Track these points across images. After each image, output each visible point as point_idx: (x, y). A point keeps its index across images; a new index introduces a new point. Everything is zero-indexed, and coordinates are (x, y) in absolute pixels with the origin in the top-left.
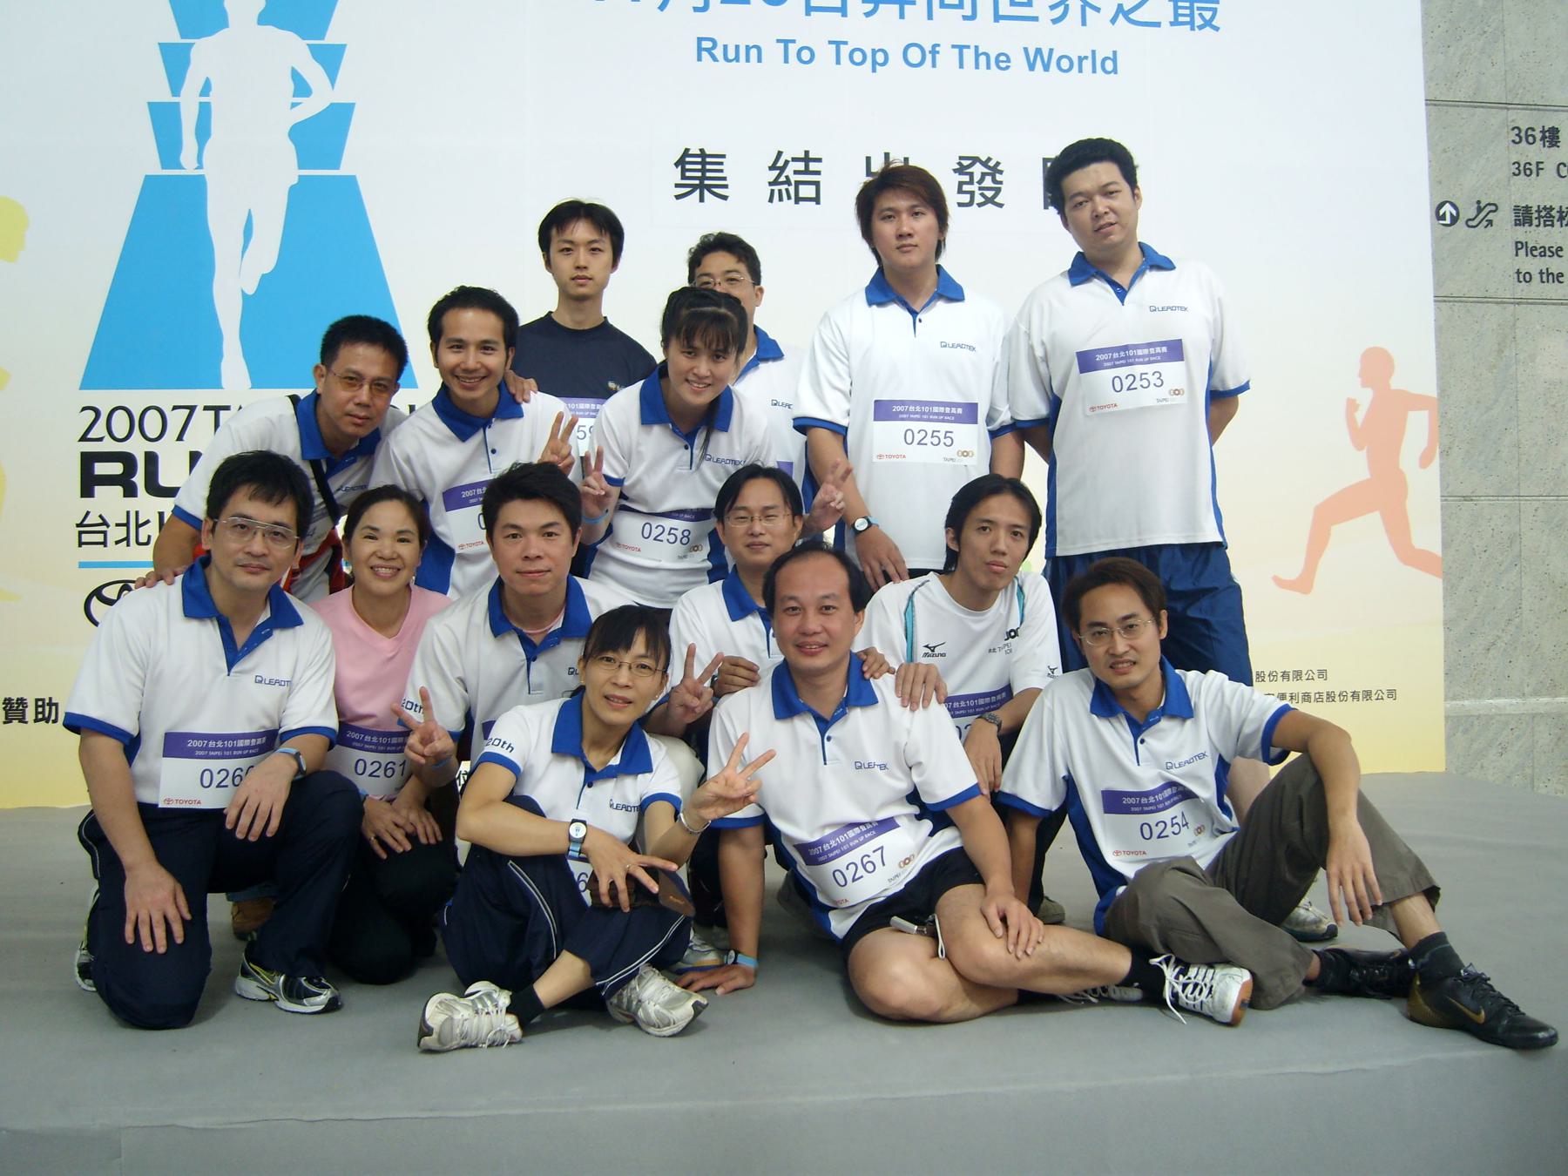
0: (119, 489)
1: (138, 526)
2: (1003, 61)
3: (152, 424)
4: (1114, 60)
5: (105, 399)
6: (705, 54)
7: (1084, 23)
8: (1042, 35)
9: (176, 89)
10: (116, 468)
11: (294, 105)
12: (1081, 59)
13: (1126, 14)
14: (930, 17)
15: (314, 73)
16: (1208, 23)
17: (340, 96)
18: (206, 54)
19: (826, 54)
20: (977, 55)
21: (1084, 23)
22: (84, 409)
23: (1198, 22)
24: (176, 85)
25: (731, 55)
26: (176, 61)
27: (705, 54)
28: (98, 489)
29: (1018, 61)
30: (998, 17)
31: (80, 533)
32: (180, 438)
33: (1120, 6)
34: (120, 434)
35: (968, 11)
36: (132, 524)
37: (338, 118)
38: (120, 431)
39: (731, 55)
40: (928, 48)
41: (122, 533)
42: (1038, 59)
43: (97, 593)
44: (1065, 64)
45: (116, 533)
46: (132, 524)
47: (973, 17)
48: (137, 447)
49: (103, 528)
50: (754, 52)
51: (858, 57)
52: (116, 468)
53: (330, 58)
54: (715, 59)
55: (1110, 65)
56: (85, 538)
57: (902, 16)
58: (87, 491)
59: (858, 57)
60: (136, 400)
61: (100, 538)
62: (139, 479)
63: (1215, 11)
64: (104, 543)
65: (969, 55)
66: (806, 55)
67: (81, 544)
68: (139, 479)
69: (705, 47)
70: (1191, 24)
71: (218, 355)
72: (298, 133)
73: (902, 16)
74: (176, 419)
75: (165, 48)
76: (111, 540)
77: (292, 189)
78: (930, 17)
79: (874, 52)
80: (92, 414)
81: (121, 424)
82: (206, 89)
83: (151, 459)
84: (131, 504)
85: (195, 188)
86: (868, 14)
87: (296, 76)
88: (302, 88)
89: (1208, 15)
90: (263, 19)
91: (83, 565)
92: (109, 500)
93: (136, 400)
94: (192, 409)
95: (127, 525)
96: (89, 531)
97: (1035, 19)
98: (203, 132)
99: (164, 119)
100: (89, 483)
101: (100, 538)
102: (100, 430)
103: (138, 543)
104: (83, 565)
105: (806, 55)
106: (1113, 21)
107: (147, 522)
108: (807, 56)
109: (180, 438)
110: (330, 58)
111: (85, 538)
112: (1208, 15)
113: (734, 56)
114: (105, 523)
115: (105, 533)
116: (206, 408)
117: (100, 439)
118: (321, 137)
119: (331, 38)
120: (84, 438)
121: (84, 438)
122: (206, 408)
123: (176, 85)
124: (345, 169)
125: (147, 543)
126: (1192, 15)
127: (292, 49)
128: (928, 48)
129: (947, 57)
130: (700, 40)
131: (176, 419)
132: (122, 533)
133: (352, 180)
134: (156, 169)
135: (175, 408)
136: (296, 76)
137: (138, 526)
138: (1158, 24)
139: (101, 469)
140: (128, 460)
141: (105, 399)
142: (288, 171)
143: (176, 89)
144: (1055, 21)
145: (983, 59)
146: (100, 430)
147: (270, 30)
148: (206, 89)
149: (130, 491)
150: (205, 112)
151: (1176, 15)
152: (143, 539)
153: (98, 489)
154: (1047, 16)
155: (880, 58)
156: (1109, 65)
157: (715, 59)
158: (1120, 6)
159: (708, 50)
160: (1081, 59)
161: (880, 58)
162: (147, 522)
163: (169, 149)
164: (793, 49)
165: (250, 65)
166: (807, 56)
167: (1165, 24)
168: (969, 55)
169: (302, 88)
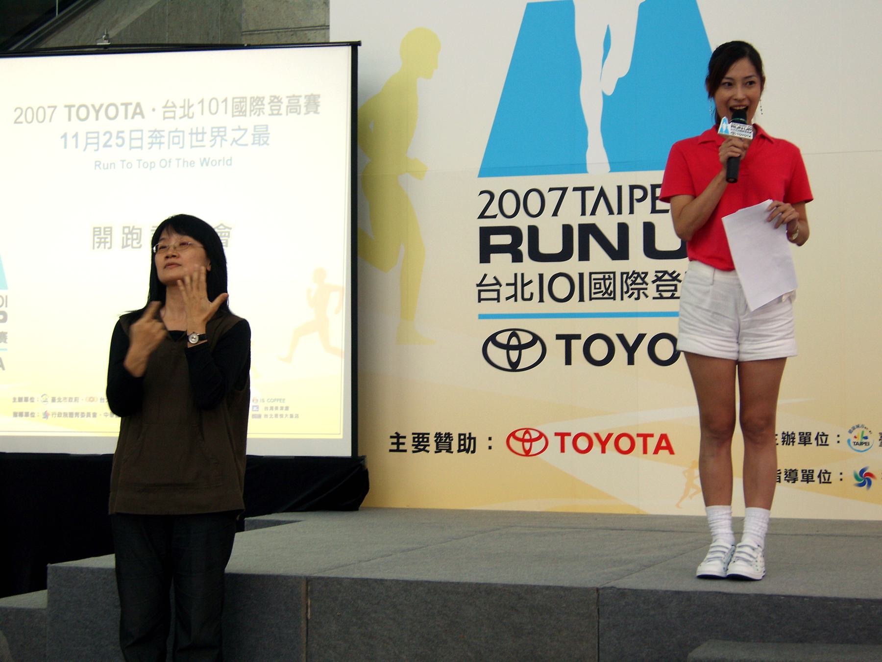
0: (509, 256)
1: (523, 285)
3: (534, 203)
5: (497, 185)
10: (506, 239)
22: (482, 193)
28: (493, 256)
31: (480, 291)
32: (555, 214)
36: (519, 283)
38: (509, 210)
41: (511, 291)
43: (492, 339)
48: (522, 222)
49: (497, 287)
52: (506, 240)
56: (484, 295)
58: (485, 258)
60: (521, 184)
61: (494, 295)
62: (524, 248)
64: (498, 299)
67: (480, 300)
68: (524, 248)
74: (552, 199)
80: (487, 197)
81: (509, 204)
83: (534, 231)
84: (518, 268)
91: (482, 317)
92: (501, 264)
93: (521, 184)
94: (564, 190)
95: (515, 284)
96: (486, 289)
100: (486, 252)
101: (494, 295)
102: (494, 209)
103: (523, 299)
104: (482, 317)
107: (531, 282)
109: (555, 214)
111: (484, 295)
114: (498, 283)
115: (498, 291)
116: (575, 189)
117: (495, 217)
120: (482, 216)
121: (482, 216)
122: (575, 189)
131: (552, 199)
132: (511, 291)
135: (551, 190)
139: (495, 240)
140: (515, 232)
141: (497, 185)
146: (494, 209)
149: (517, 258)
152: (527, 296)
153: (493, 256)
162: (531, 282)
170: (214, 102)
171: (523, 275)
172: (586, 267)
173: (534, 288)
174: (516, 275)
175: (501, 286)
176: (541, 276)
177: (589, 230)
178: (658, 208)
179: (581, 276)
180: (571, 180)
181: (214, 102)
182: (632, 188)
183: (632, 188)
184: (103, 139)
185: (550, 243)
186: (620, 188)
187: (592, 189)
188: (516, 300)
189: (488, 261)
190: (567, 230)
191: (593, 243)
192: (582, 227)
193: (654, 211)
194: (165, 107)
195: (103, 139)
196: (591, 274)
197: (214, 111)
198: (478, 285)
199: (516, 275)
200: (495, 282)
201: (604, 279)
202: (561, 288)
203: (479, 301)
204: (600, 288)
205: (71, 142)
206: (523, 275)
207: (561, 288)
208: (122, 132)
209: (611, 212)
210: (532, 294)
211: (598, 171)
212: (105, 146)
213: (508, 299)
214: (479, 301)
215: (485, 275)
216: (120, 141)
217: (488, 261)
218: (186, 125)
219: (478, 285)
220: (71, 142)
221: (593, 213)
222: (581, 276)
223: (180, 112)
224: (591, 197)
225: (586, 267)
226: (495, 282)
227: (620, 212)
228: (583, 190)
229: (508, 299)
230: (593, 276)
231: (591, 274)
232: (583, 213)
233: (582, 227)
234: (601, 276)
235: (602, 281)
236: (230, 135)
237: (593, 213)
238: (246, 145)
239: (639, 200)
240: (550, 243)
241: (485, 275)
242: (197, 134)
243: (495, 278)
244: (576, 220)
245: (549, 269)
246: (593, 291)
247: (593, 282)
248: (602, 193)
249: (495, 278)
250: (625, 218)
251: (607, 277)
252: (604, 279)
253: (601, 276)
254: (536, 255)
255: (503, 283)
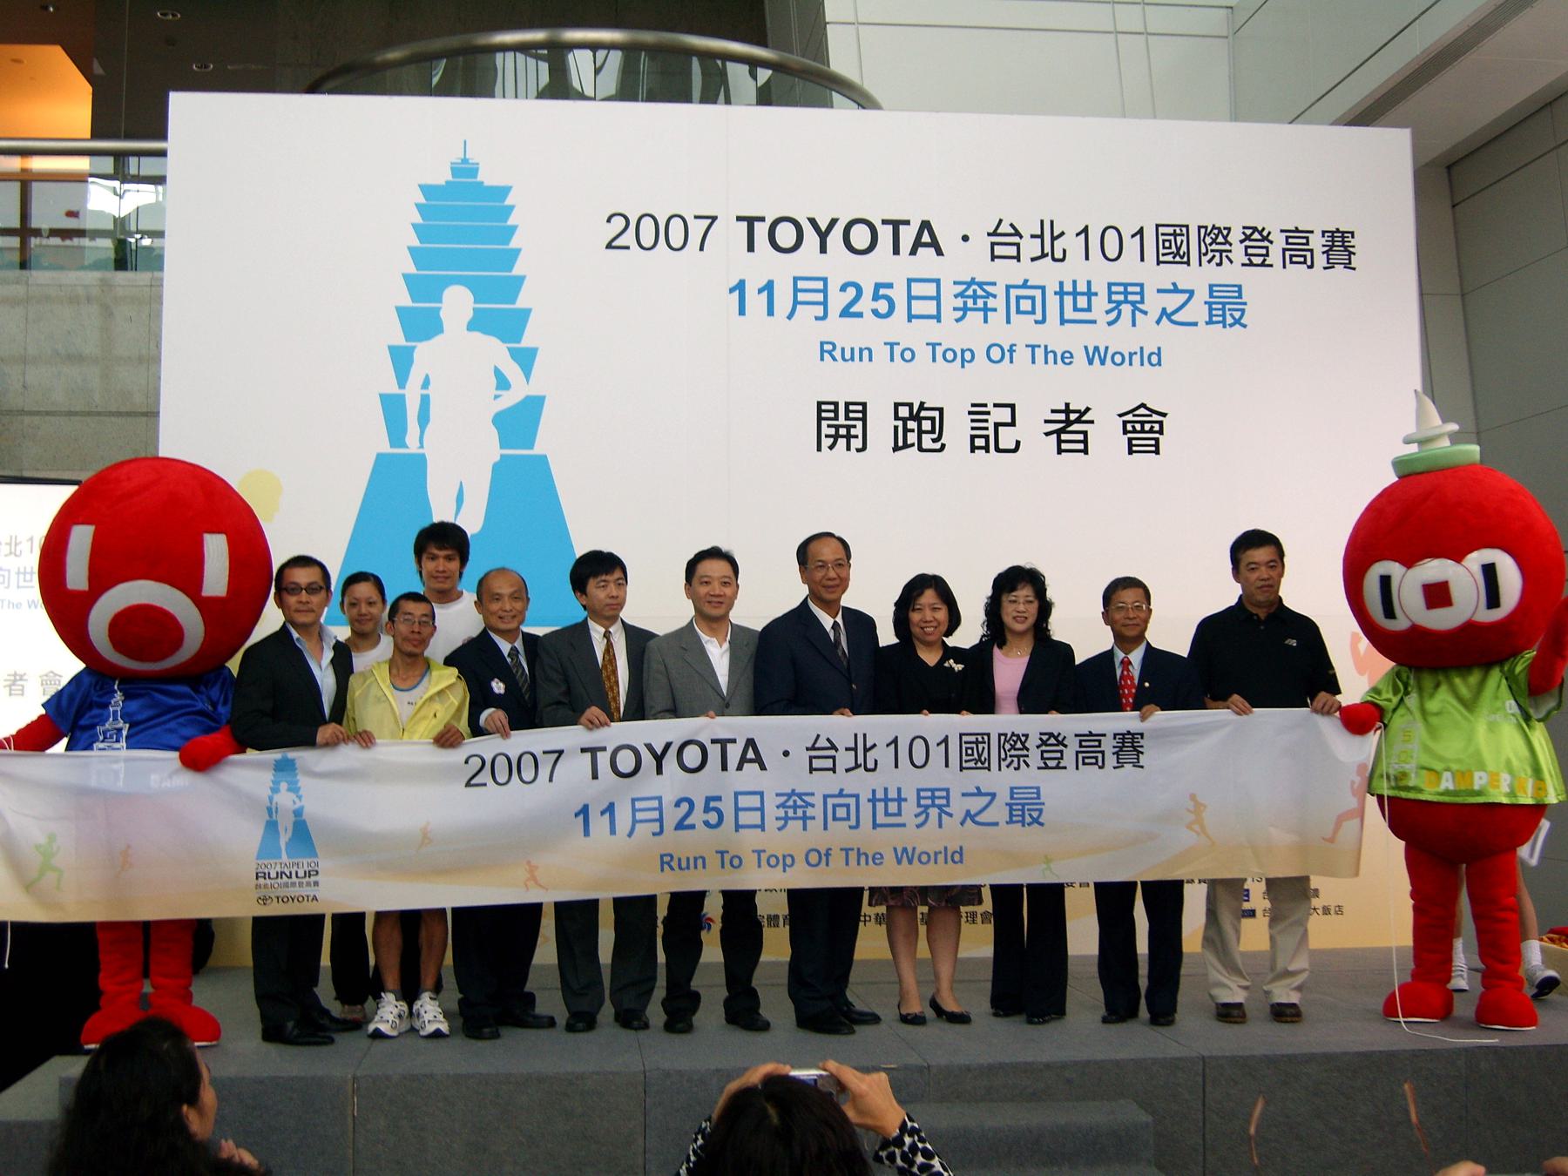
2: (1066, 358)
4: (1159, 355)
6: (826, 355)
7: (1134, 324)
8: (1099, 335)
9: (402, 385)
11: (496, 397)
12: (1131, 355)
13: (1169, 317)
14: (1008, 322)
15: (512, 371)
16: (1237, 322)
17: (533, 389)
18: (426, 354)
19: (924, 353)
20: (1046, 353)
21: (1134, 324)
23: (1229, 320)
24: (402, 381)
25: (848, 356)
26: (402, 360)
27: (826, 355)
29: (1080, 357)
30: (1063, 321)
33: (1164, 310)
35: (1039, 316)
37: (533, 406)
39: (848, 356)
40: (1006, 348)
42: (1096, 355)
44: (1118, 359)
47: (1043, 321)
50: (866, 353)
51: (950, 356)
53: (526, 359)
54: (834, 359)
55: (1155, 358)
57: (986, 321)
59: (950, 356)
63: (1243, 311)
65: (1040, 353)
66: (908, 355)
69: (827, 350)
70: (1224, 323)
72: (500, 420)
73: (986, 321)
75: (393, 350)
77: (495, 466)
78: (1008, 322)
79: (963, 351)
82: (426, 383)
85: (418, 464)
86: (957, 321)
87: (497, 372)
88: (503, 383)
89: (1237, 314)
90: (471, 326)
97: (1094, 322)
98: (424, 419)
99: (393, 408)
105: (908, 355)
106: (1158, 322)
108: (909, 356)
110: (526, 359)
112: (1237, 314)
113: (850, 356)
118: (519, 423)
119: (527, 342)
123: (402, 381)
124: (537, 450)
126: (1224, 316)
127: (494, 351)
128: (1006, 348)
129: (1022, 354)
130: (822, 344)
133: (542, 460)
134: (386, 448)
136: (497, 372)
138: (1195, 324)
142: (490, 449)
143: (402, 385)
144: (1110, 324)
145: (1051, 356)
147: (477, 335)
148: (426, 383)
150: (425, 400)
151: (1211, 315)
154: (1103, 319)
155: (968, 356)
156: (1154, 359)
157: (834, 359)
158: (1164, 310)
159: (830, 352)
160: (1131, 355)
161: (968, 356)
163: (396, 431)
164: (898, 351)
165: (461, 363)
166: (909, 356)
167: (1202, 324)
168: (1040, 353)
169: (503, 383)
170: (1111, 234)
181: (1111, 234)
184: (838, 301)
194: (994, 234)
195: (838, 301)
197: (1112, 254)
205: (756, 302)
208: (890, 286)
212: (846, 313)
216: (883, 306)
218: (1047, 274)
220: (756, 302)
223: (1030, 247)
236: (1154, 303)
238: (1195, 324)
242: (1075, 294)
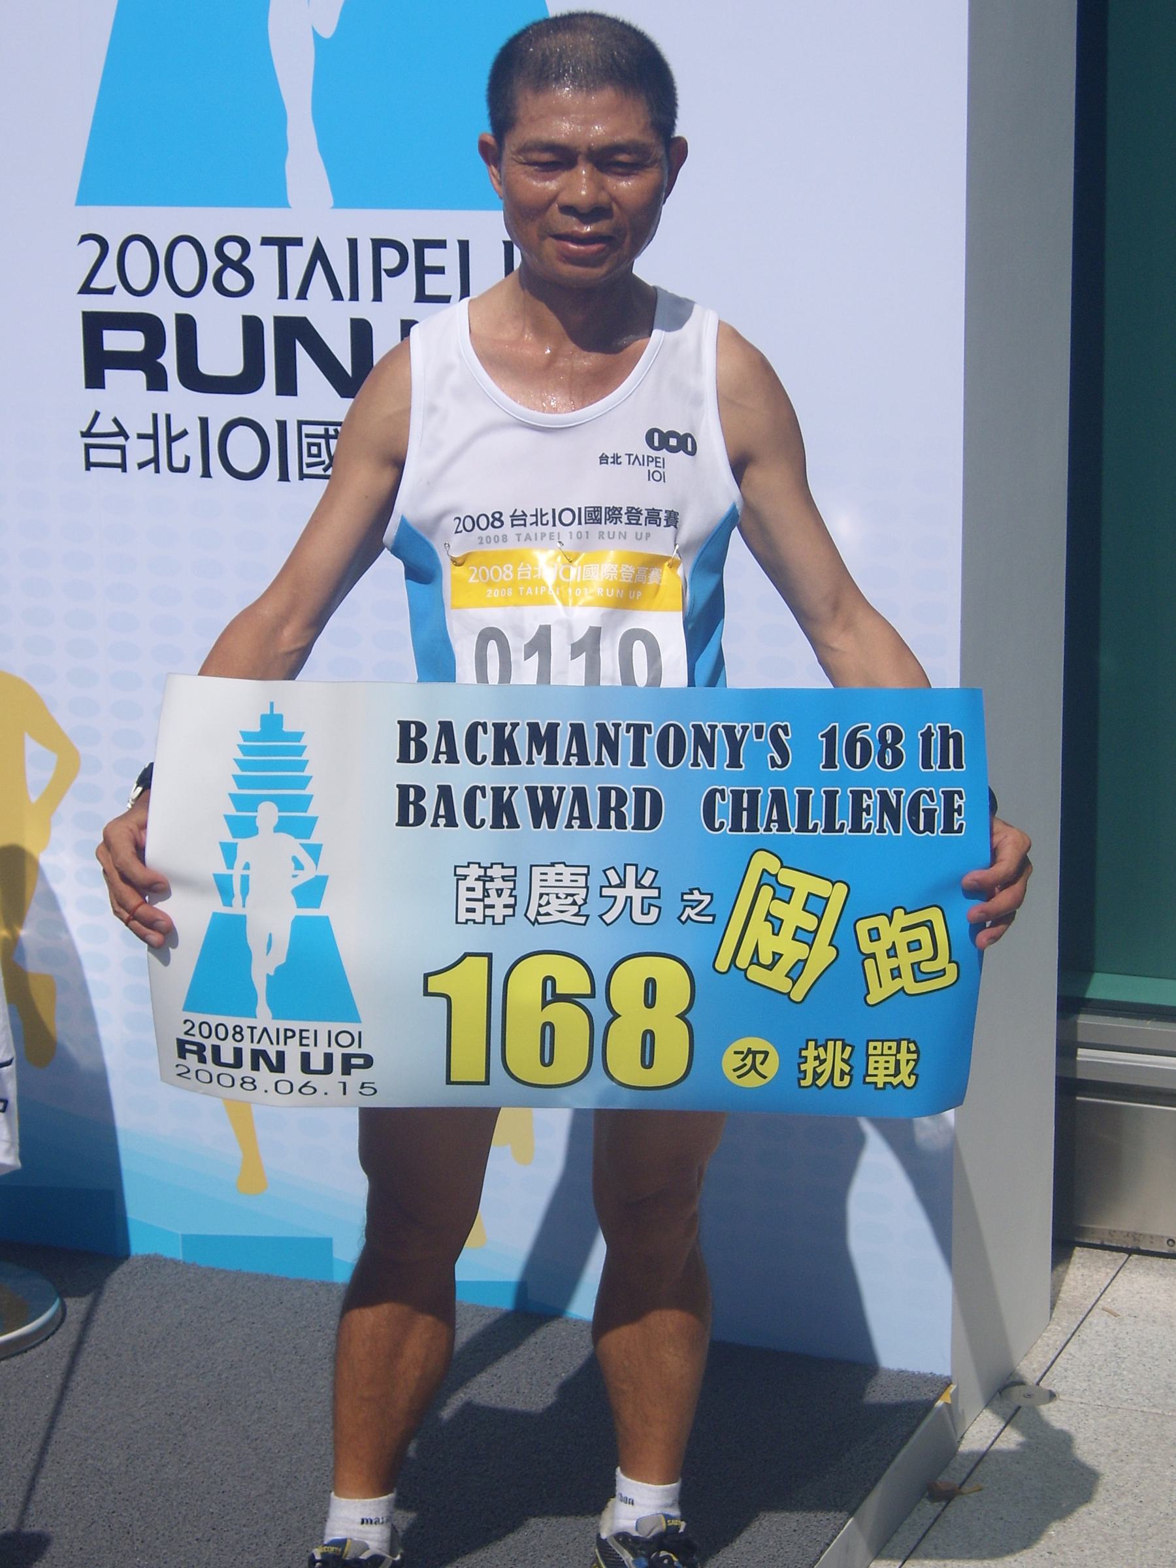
0: (139, 377)
1: (171, 440)
5: (115, 223)
10: (133, 341)
22: (84, 238)
31: (88, 447)
34: (139, 283)
36: (163, 435)
38: (139, 279)
45: (140, 450)
46: (163, 435)
48: (163, 305)
49: (120, 440)
52: (133, 341)
56: (96, 455)
58: (94, 380)
60: (162, 224)
61: (115, 456)
62: (169, 360)
67: (89, 465)
68: (169, 360)
71: (282, 149)
76: (131, 464)
80: (94, 248)
83: (186, 325)
95: (154, 437)
101: (115, 456)
102: (107, 276)
103: (172, 468)
107: (184, 433)
111: (96, 455)
114: (122, 433)
115: (122, 449)
116: (266, 241)
117: (110, 291)
120: (86, 289)
121: (86, 289)
122: (266, 241)
125: (185, 469)
137: (171, 440)
140: (149, 325)
146: (107, 276)
149: (157, 381)
152: (179, 462)
153: (109, 374)
162: (184, 433)
171: (168, 417)
172: (290, 409)
173: (190, 447)
174: (155, 417)
175: (127, 437)
176: (204, 422)
177: (295, 331)
178: (429, 291)
179: (282, 426)
180: (255, 223)
182: (378, 244)
183: (378, 244)
185: (221, 354)
186: (353, 244)
187: (298, 242)
188: (157, 471)
189: (102, 386)
190: (252, 326)
191: (303, 359)
192: (279, 322)
193: (422, 297)
196: (301, 424)
198: (84, 435)
199: (155, 417)
200: (116, 429)
201: (327, 437)
202: (244, 449)
203: (88, 469)
204: (319, 455)
206: (168, 417)
207: (244, 449)
209: (338, 296)
210: (188, 459)
211: (313, 209)
213: (141, 466)
214: (88, 469)
215: (97, 414)
217: (102, 386)
219: (84, 435)
221: (302, 295)
222: (282, 426)
224: (298, 259)
225: (290, 409)
226: (116, 429)
227: (354, 296)
228: (282, 244)
229: (141, 466)
230: (306, 429)
231: (301, 424)
232: (283, 294)
233: (279, 322)
234: (320, 430)
235: (322, 441)
237: (302, 295)
239: (392, 273)
240: (221, 354)
241: (97, 414)
243: (116, 421)
244: (266, 305)
245: (222, 408)
246: (306, 460)
247: (305, 441)
248: (319, 254)
249: (116, 421)
250: (365, 308)
251: (332, 432)
252: (327, 437)
253: (320, 430)
254: (194, 379)
255: (132, 434)
